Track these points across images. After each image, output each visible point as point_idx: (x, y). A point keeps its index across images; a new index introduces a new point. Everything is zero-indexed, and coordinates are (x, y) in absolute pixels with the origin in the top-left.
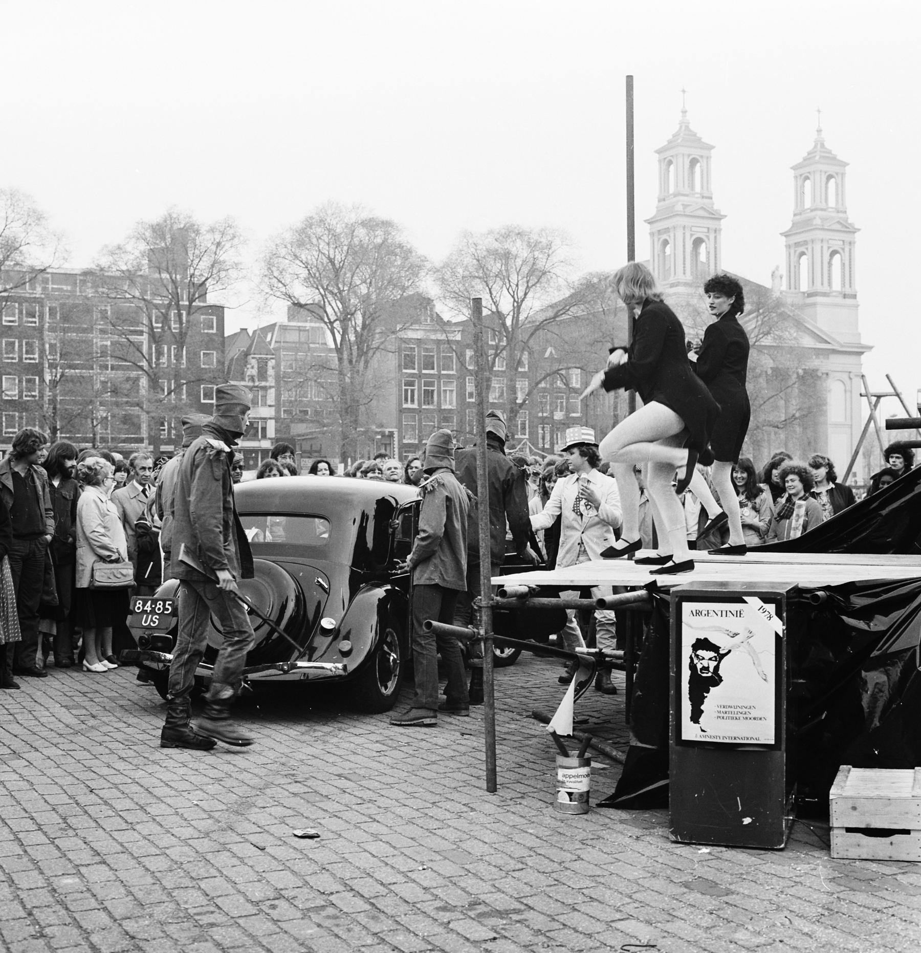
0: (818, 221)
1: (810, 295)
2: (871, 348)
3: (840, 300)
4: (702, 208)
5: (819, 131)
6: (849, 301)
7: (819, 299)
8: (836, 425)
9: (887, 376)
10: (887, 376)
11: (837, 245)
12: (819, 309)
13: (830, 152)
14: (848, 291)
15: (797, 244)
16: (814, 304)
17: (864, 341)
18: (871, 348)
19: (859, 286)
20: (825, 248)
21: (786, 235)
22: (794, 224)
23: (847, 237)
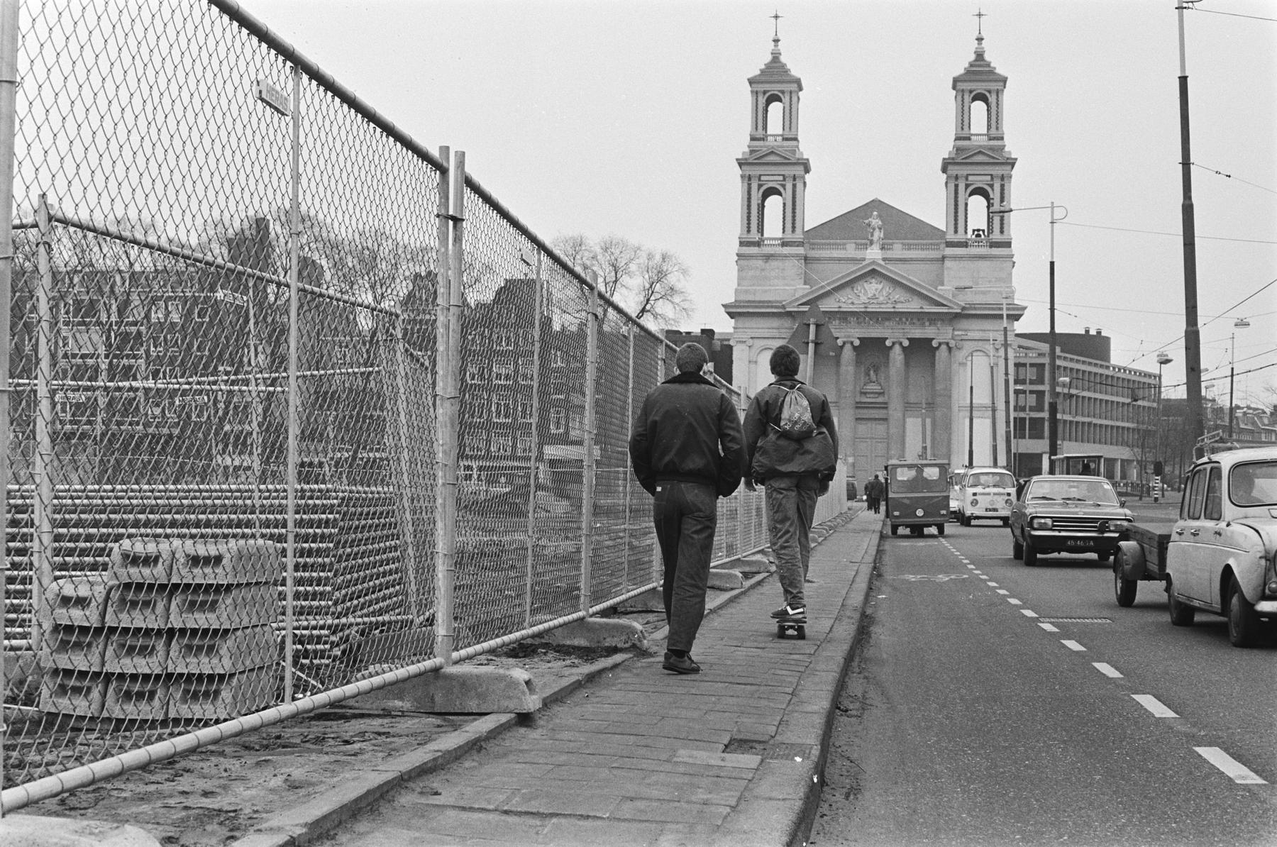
6: (995, 251)
12: (948, 263)
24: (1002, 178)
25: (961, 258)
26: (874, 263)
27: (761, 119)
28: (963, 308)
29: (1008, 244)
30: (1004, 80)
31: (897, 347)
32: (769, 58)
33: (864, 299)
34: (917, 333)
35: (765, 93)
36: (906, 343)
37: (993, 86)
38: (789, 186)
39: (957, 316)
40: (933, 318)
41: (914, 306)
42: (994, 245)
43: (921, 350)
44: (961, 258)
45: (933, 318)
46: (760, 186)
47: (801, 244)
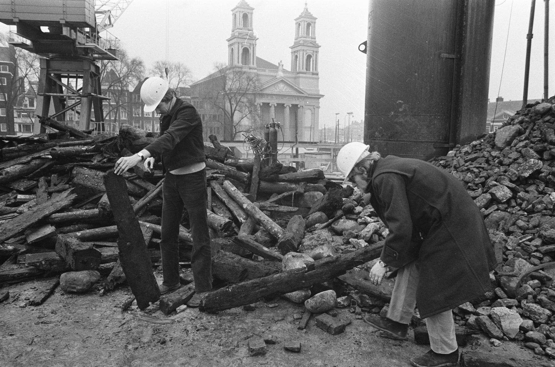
0: (302, 42)
1: (298, 73)
3: (311, 76)
5: (306, 4)
6: (314, 76)
7: (301, 75)
8: (306, 128)
11: (310, 53)
13: (310, 13)
14: (314, 71)
15: (295, 52)
16: (299, 77)
17: (321, 93)
18: (323, 96)
20: (305, 53)
21: (292, 48)
22: (295, 43)
23: (315, 49)
24: (316, 52)
25: (305, 77)
28: (309, 95)
29: (317, 74)
31: (288, 107)
33: (278, 90)
34: (294, 103)
36: (291, 106)
37: (313, 21)
38: (252, 48)
39: (306, 97)
40: (298, 97)
42: (313, 74)
43: (295, 108)
44: (305, 77)
46: (242, 46)
47: (255, 69)
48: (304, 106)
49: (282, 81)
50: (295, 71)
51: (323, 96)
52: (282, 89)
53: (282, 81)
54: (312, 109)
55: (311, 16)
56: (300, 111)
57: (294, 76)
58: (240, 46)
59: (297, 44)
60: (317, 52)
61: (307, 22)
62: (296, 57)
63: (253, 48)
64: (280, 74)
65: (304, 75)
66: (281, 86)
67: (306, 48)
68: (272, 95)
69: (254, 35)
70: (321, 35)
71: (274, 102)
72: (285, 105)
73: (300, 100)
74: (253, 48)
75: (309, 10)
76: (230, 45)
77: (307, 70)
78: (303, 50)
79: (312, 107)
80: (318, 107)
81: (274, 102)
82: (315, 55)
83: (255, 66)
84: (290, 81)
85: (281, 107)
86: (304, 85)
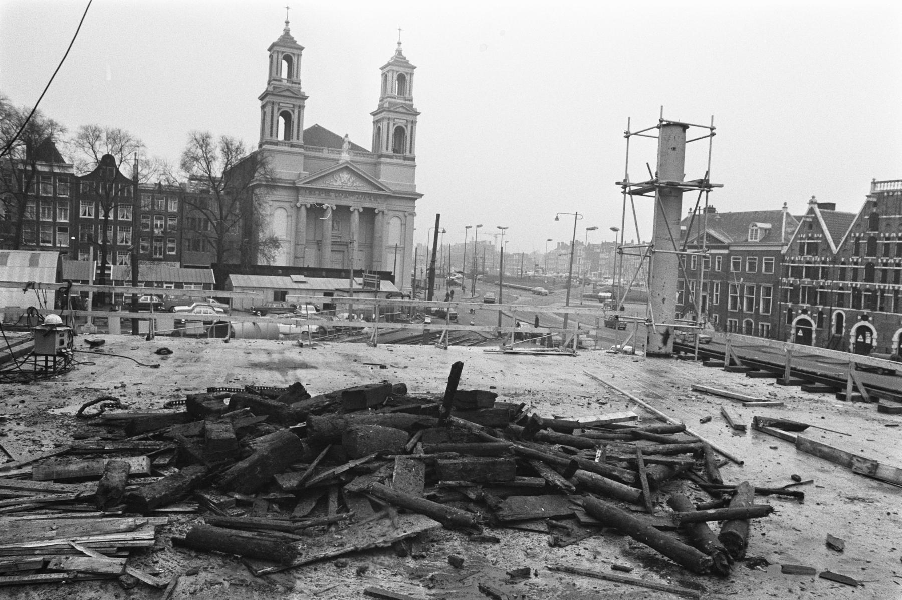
2: (421, 196)
3: (401, 161)
4: (287, 90)
6: (407, 162)
7: (383, 160)
9: (438, 216)
10: (438, 216)
11: (401, 123)
12: (382, 167)
16: (380, 163)
17: (418, 191)
18: (421, 196)
19: (418, 151)
20: (391, 125)
21: (374, 114)
23: (410, 118)
24: (412, 122)
26: (347, 162)
27: (274, 68)
28: (394, 193)
29: (413, 159)
30: (302, 48)
31: (356, 212)
32: (282, 33)
33: (339, 183)
34: (368, 205)
35: (283, 52)
36: (361, 210)
37: (408, 70)
38: (296, 111)
39: (389, 197)
40: (376, 197)
41: (367, 189)
43: (369, 215)
45: (376, 197)
46: (279, 109)
47: (301, 147)
48: (386, 212)
49: (346, 168)
50: (377, 153)
51: (421, 196)
52: (344, 181)
53: (346, 168)
54: (403, 218)
55: (407, 62)
56: (379, 218)
57: (373, 160)
58: (276, 109)
59: (381, 109)
60: (414, 123)
61: (400, 74)
62: (379, 128)
63: (299, 112)
64: (345, 157)
65: (388, 160)
66: (345, 176)
67: (391, 115)
68: (327, 192)
69: (302, 90)
70: (421, 94)
71: (329, 204)
72: (352, 209)
73: (379, 201)
74: (299, 112)
75: (404, 54)
76: (263, 107)
77: (395, 151)
78: (389, 119)
79: (401, 214)
80: (413, 215)
81: (329, 204)
82: (409, 127)
83: (301, 142)
84: (362, 169)
85: (342, 212)
86: (389, 176)
